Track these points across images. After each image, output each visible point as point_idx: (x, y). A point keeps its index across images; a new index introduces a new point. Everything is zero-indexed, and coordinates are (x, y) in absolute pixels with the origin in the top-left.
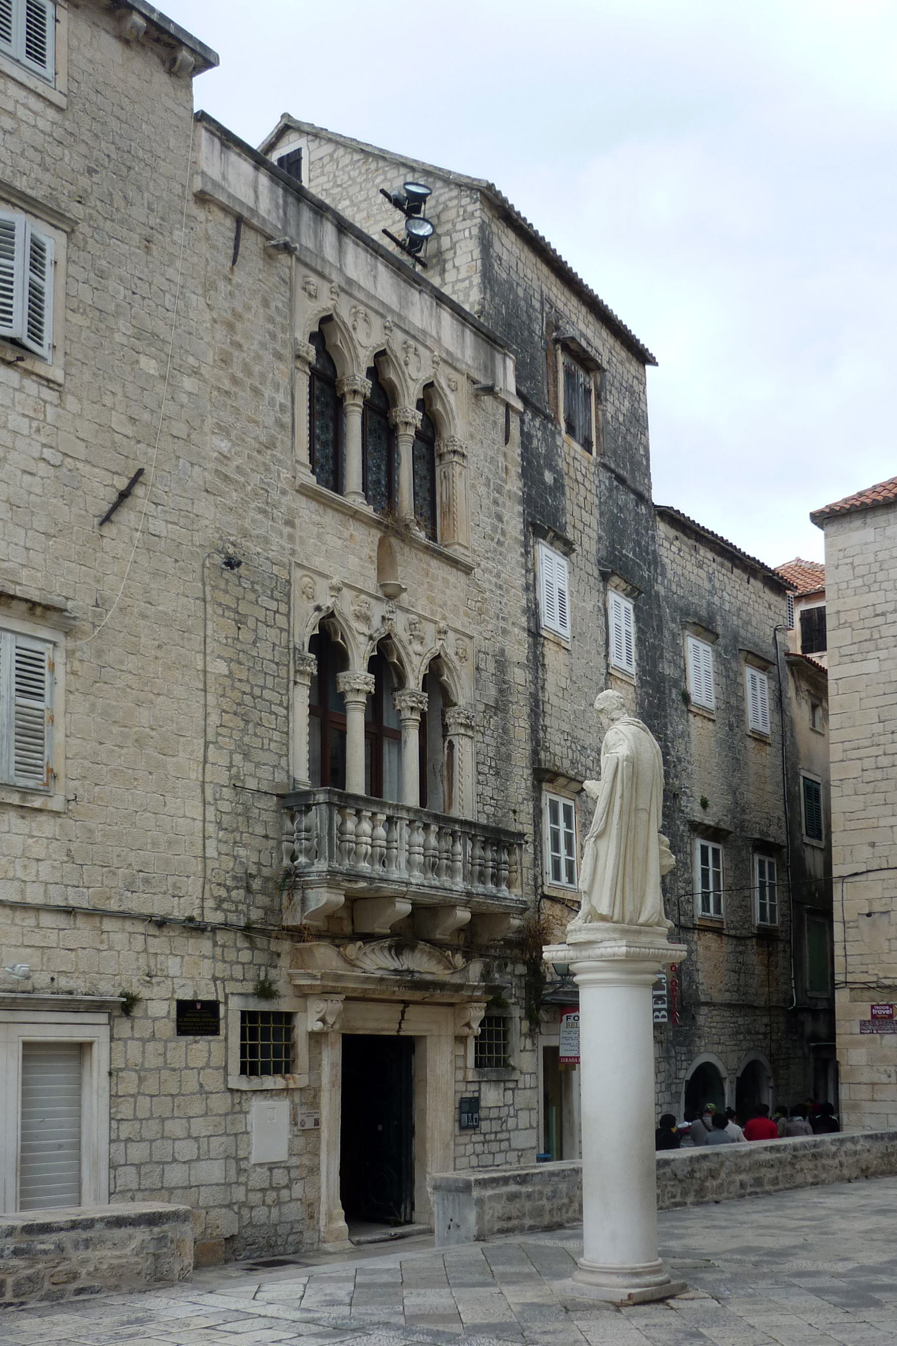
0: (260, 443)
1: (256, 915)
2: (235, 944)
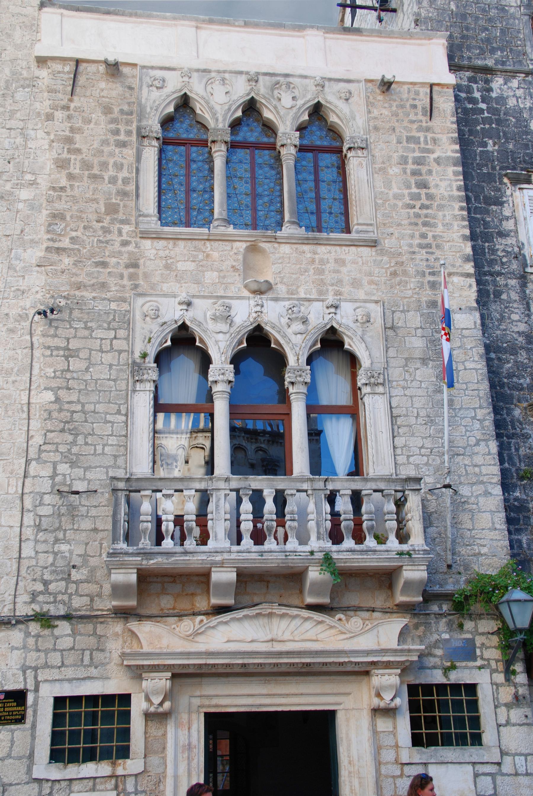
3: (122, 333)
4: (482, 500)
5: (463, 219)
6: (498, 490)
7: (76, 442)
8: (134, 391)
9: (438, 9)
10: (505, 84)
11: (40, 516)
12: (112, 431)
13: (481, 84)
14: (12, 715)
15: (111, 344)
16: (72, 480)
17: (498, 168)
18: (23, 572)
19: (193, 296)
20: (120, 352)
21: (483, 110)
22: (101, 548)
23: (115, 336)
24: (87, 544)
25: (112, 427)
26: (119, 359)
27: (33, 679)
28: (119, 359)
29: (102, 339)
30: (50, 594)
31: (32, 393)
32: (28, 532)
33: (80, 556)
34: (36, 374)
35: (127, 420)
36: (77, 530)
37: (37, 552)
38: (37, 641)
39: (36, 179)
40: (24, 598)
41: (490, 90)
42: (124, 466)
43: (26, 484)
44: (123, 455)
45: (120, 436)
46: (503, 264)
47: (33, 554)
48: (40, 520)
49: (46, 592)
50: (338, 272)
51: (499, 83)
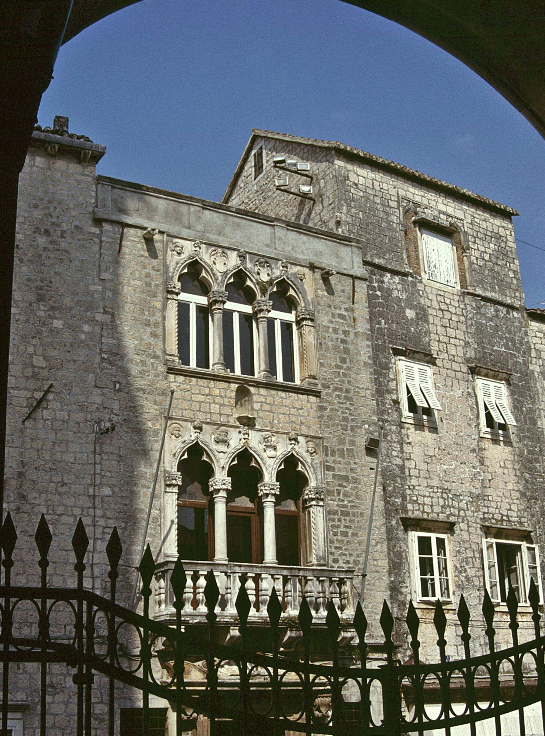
9: (352, 216)
13: (378, 277)
17: (387, 341)
41: (383, 282)
46: (389, 414)
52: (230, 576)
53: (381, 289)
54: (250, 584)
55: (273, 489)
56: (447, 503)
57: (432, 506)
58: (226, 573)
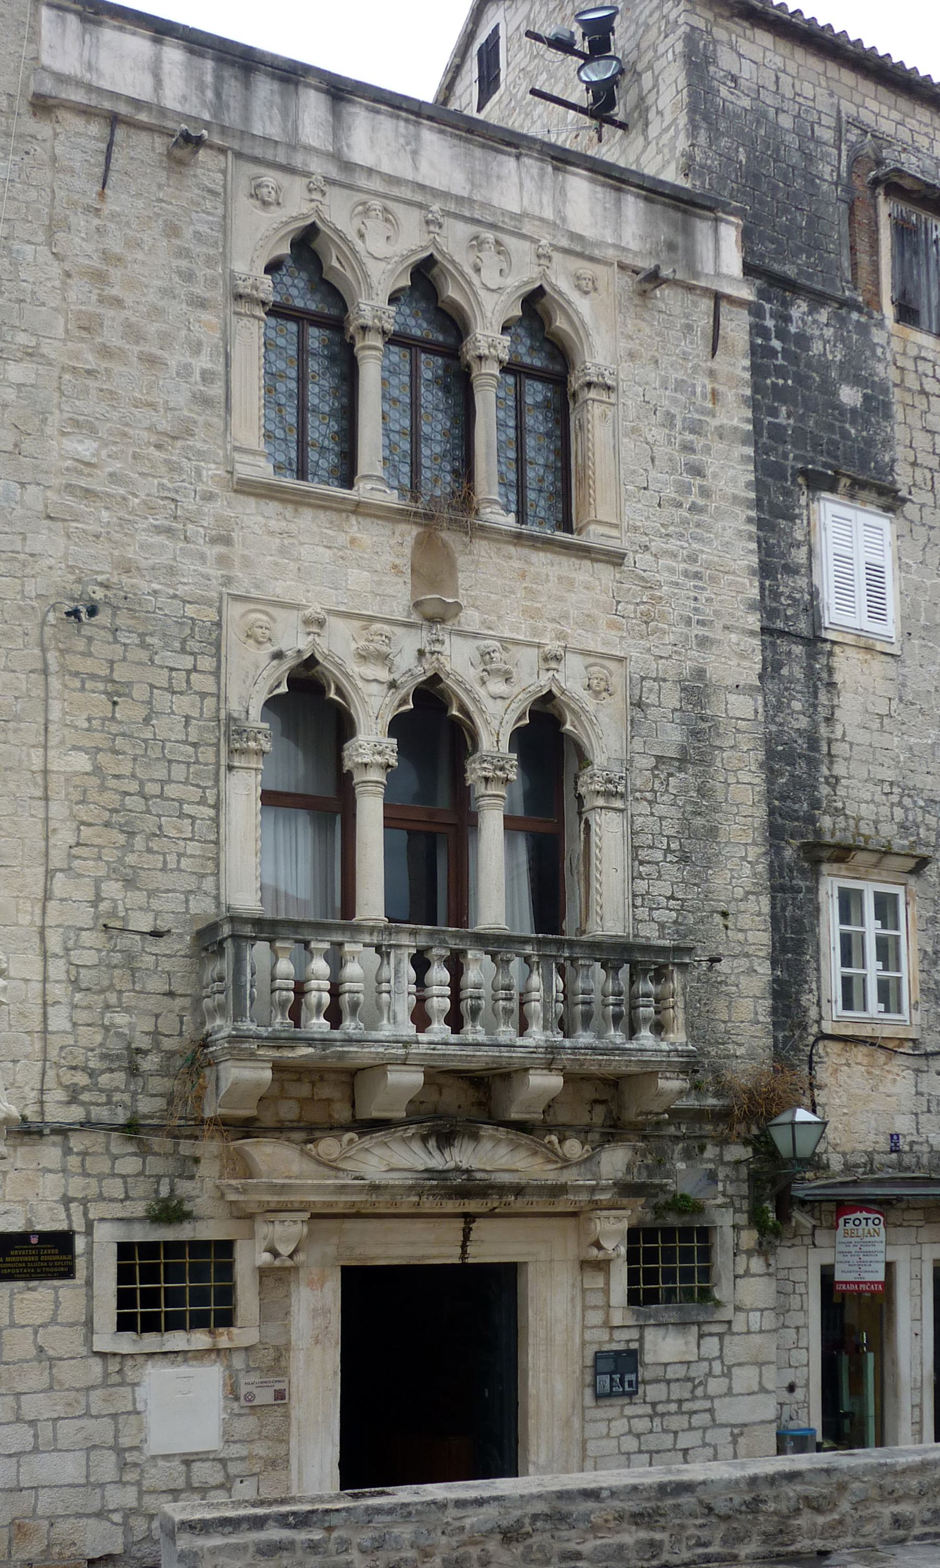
0: (158, 433)
1: (146, 1106)
2: (107, 1149)
3: (206, 663)
4: (743, 980)
5: (750, 538)
6: (764, 969)
7: (133, 846)
8: (230, 768)
10: (810, 313)
11: (77, 966)
12: (193, 831)
14: (54, 1266)
15: (188, 681)
16: (127, 910)
18: (53, 1053)
19: (329, 612)
20: (203, 695)
21: (777, 352)
22: (182, 1023)
23: (195, 666)
24: (157, 1016)
25: (193, 824)
26: (201, 709)
27: (81, 1217)
28: (201, 709)
29: (172, 669)
30: (101, 1091)
31: (52, 753)
32: (58, 991)
33: (147, 1033)
34: (56, 719)
35: (218, 816)
36: (142, 992)
37: (75, 1025)
38: (83, 1160)
39: (38, 345)
40: (60, 1095)
41: (788, 319)
42: (214, 892)
43: (49, 911)
44: (211, 874)
45: (206, 842)
47: (68, 1026)
48: (78, 973)
49: (94, 1087)
50: (561, 599)
51: (801, 310)
52: (388, 954)
53: (782, 334)
54: (439, 974)
55: (502, 769)
56: (911, 818)
57: (876, 822)
58: (378, 949)
